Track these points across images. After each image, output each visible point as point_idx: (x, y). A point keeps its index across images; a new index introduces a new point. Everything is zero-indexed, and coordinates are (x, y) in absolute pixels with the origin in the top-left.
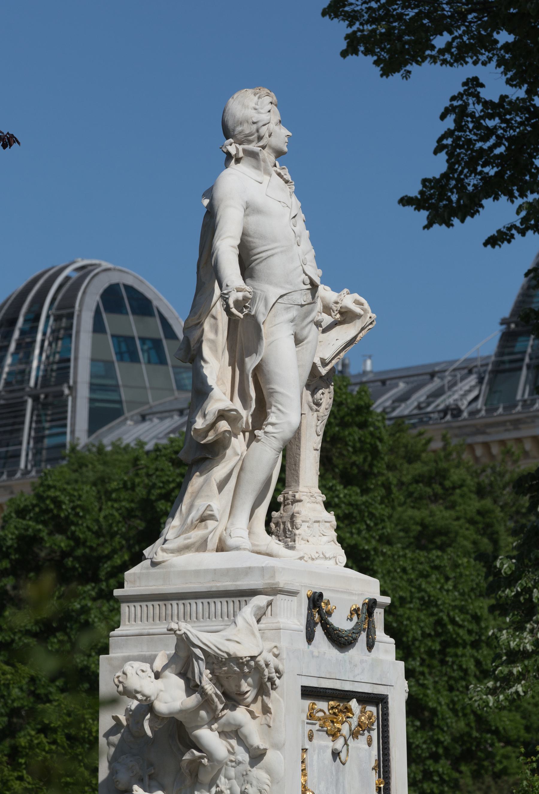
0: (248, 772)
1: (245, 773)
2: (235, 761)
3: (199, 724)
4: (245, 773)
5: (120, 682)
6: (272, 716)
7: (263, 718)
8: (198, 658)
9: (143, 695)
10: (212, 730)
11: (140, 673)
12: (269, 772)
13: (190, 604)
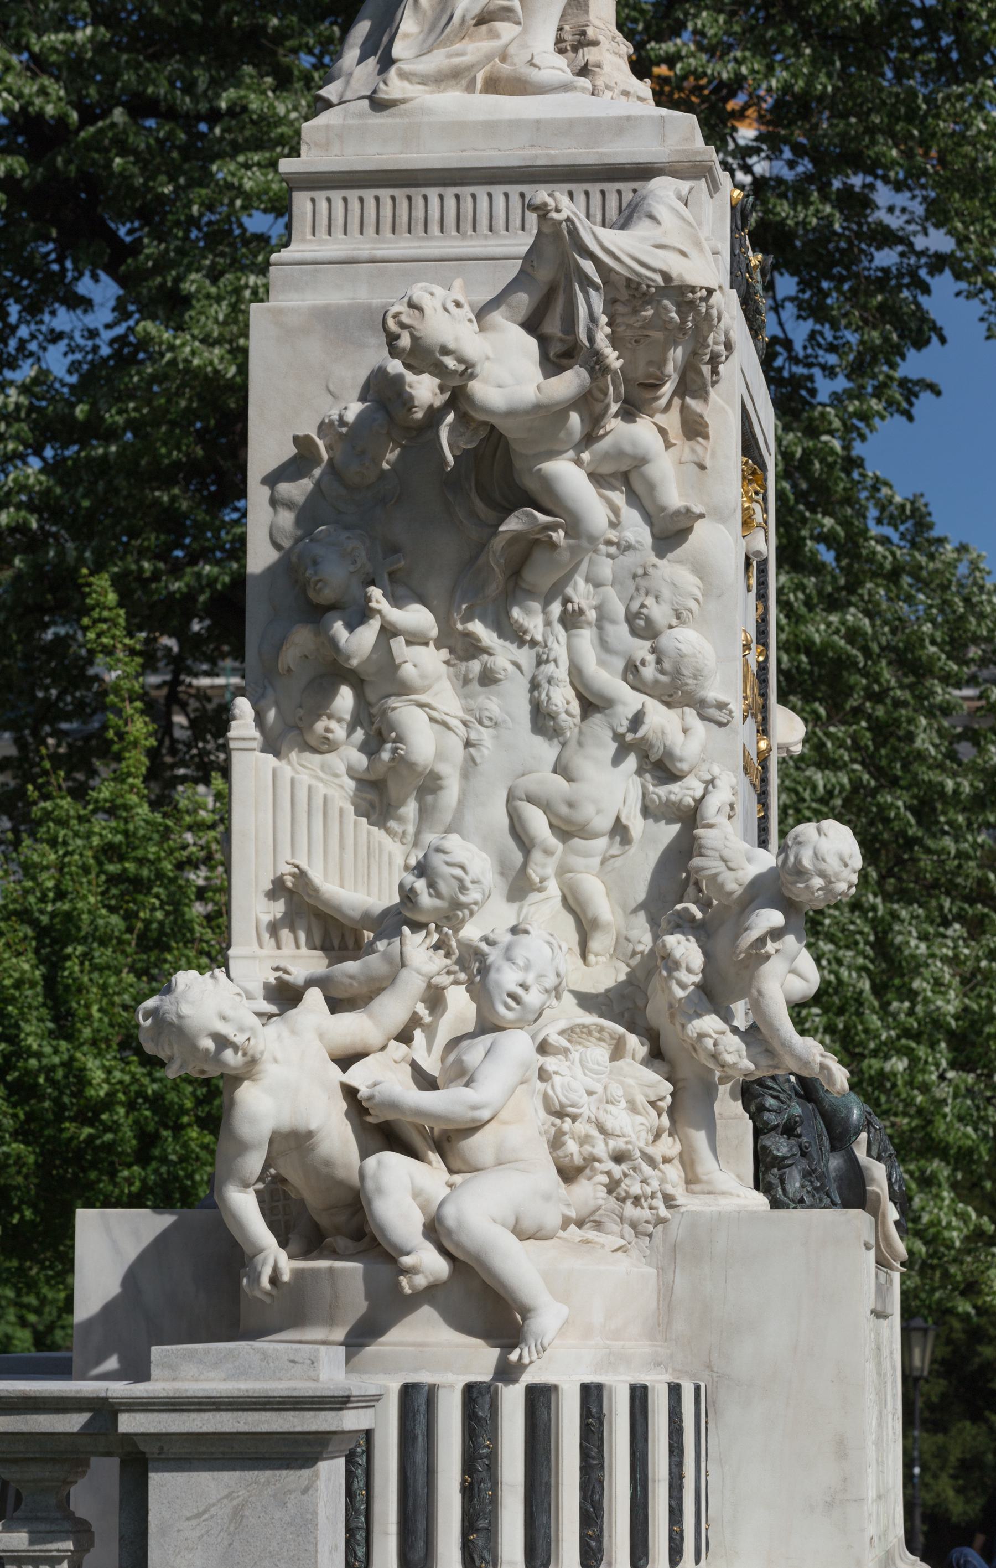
0: (650, 570)
1: (640, 571)
2: (618, 544)
3: (556, 448)
4: (640, 571)
5: (403, 326)
6: (710, 444)
7: (687, 450)
8: (586, 282)
9: (460, 360)
10: (578, 462)
11: (451, 306)
12: (700, 570)
13: (474, 196)
